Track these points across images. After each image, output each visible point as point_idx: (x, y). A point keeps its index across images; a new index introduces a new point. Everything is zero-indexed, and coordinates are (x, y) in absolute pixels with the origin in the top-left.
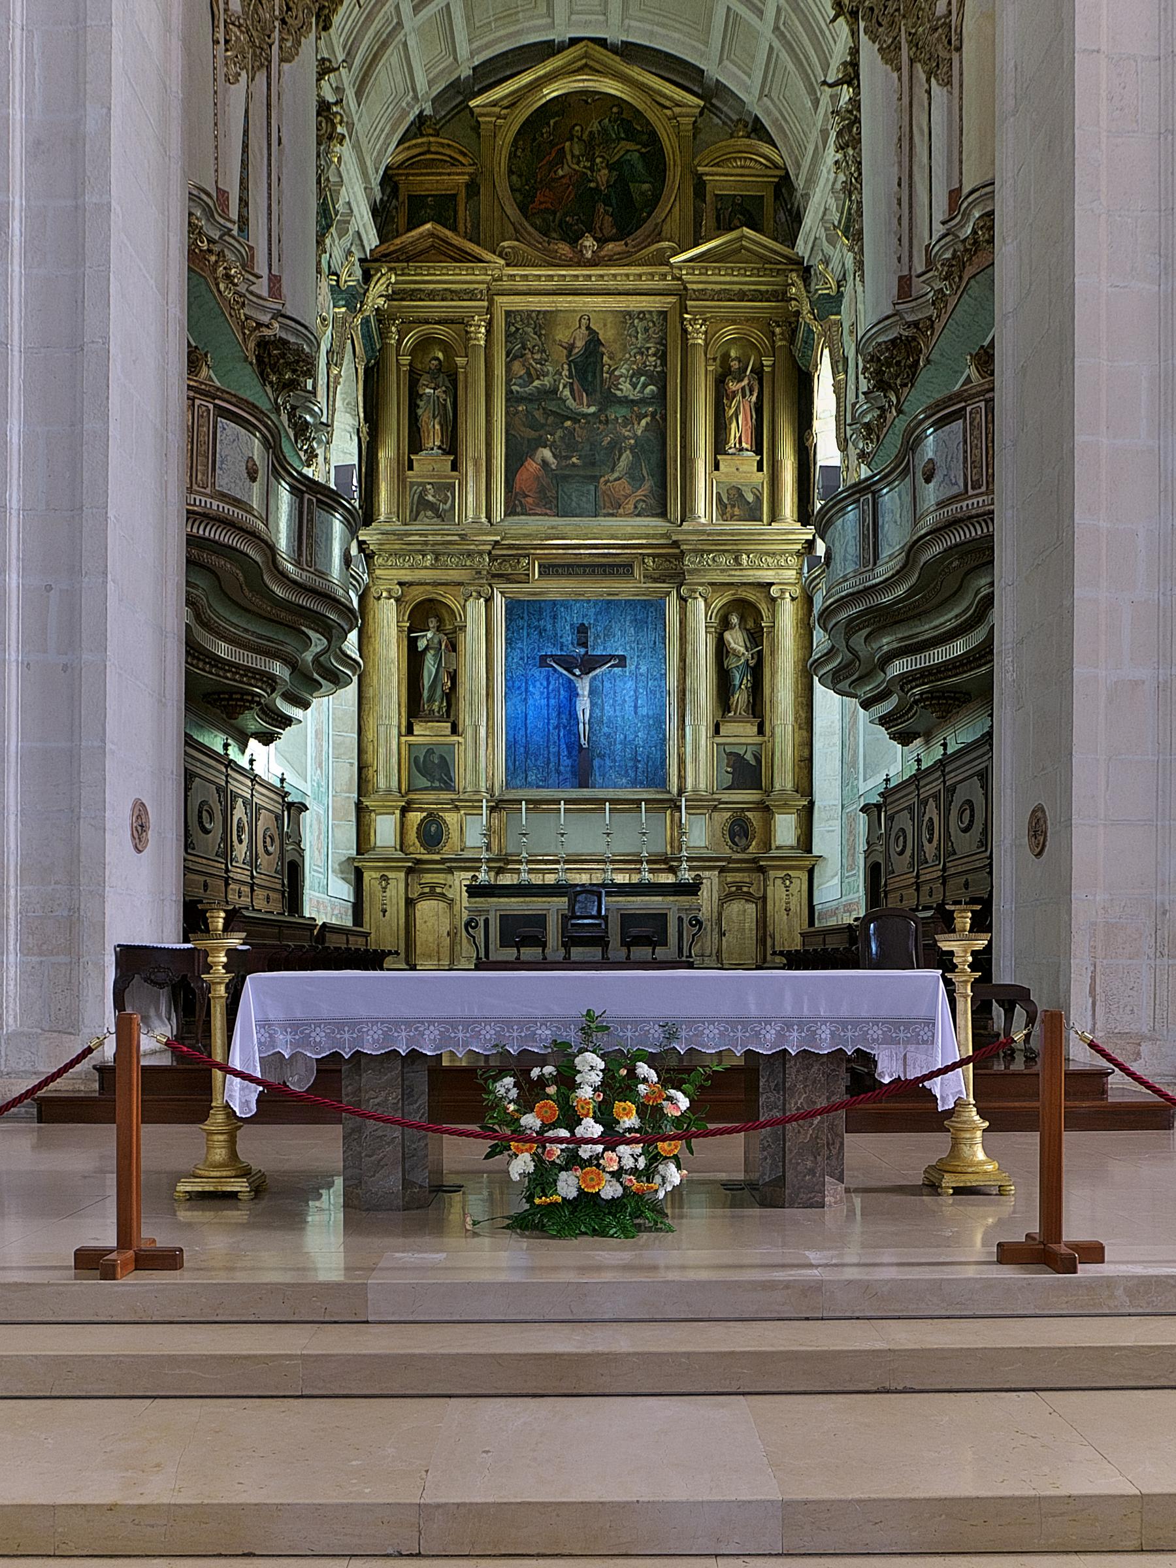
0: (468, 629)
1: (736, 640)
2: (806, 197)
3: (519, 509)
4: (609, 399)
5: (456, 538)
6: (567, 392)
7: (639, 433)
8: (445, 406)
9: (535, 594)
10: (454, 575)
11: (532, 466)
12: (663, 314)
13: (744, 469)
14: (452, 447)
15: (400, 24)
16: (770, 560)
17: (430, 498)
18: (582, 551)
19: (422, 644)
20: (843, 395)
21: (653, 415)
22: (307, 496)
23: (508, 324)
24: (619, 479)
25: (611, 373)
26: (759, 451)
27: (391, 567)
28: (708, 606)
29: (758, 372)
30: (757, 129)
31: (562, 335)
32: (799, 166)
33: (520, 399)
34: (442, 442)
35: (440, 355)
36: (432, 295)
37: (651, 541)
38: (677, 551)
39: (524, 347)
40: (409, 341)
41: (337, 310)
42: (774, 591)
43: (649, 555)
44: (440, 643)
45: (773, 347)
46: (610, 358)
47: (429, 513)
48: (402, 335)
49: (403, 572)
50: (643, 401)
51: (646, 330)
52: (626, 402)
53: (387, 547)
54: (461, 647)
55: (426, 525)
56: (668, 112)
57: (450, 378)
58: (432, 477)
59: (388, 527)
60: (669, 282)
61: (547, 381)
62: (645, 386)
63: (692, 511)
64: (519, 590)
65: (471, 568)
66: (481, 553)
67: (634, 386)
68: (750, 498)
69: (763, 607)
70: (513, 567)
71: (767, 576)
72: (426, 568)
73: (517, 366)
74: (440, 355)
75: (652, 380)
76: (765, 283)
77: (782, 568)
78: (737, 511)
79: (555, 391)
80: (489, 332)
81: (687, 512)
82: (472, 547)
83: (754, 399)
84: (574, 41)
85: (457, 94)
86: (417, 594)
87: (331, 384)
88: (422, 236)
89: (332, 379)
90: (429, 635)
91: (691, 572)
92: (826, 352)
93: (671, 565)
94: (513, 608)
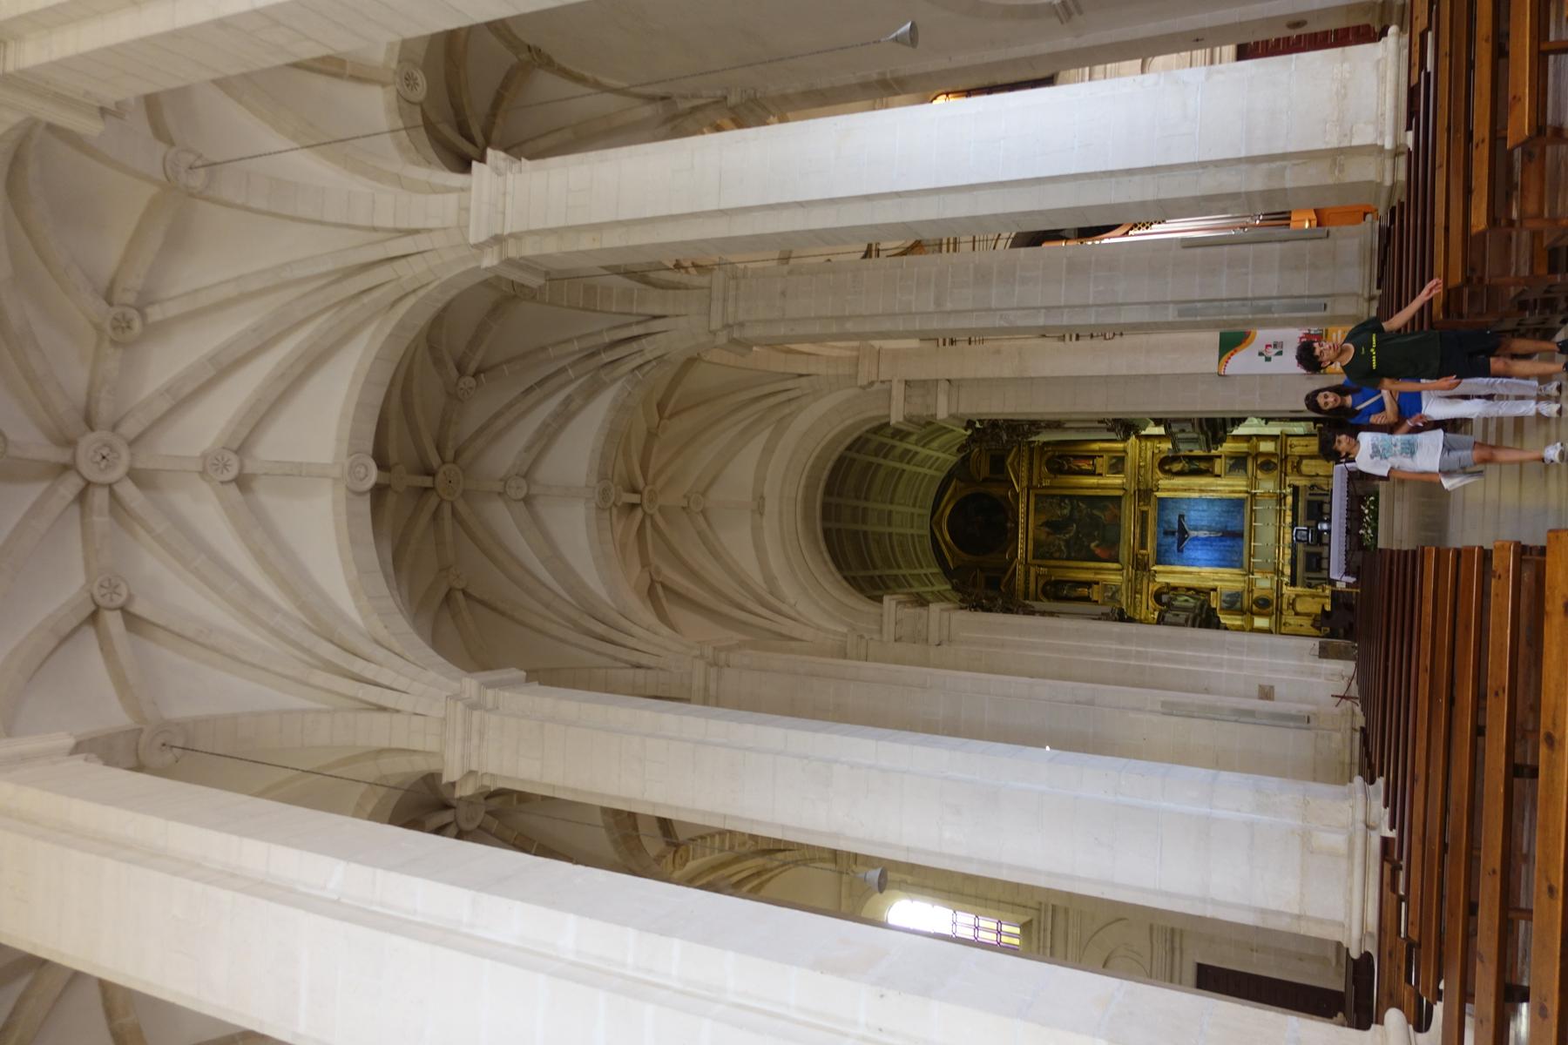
1: (1177, 467)
4: (1070, 519)
11: (1098, 551)
13: (1102, 464)
14: (1088, 584)
26: (1093, 457)
57: (1060, 583)
71: (1149, 454)
79: (1067, 542)
85: (948, 573)
94: (1158, 563)
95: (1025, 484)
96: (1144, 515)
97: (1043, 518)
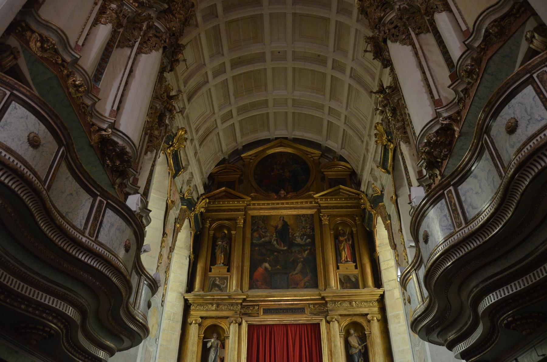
0: (231, 338)
1: (354, 341)
2: (362, 175)
3: (255, 287)
4: (291, 244)
5: (227, 297)
6: (275, 243)
7: (305, 256)
8: (226, 249)
9: (261, 321)
10: (225, 314)
11: (261, 270)
12: (312, 215)
13: (349, 269)
14: (228, 263)
15: (217, 127)
16: (365, 304)
17: (217, 282)
18: (282, 303)
19: (209, 345)
20: (390, 229)
21: (310, 250)
22: (99, 198)
23: (252, 220)
24: (297, 274)
25: (293, 235)
26: (354, 261)
27: (198, 310)
28: (340, 325)
29: (351, 233)
30: (342, 159)
31: (273, 223)
32: (357, 167)
33: (256, 245)
34: (224, 261)
35: (226, 232)
36: (224, 211)
37: (312, 297)
38: (324, 302)
39: (258, 227)
40: (214, 225)
41: (183, 207)
42: (369, 317)
43: (312, 304)
44: (217, 345)
45: (356, 225)
46: (292, 230)
47: (217, 289)
48: (211, 224)
49: (203, 312)
50: (306, 245)
51: (306, 220)
52: (299, 245)
53: (196, 302)
54: (226, 346)
55: (216, 294)
56: (310, 156)
57: (229, 239)
58: (219, 274)
59: (198, 293)
60: (314, 204)
61: (267, 239)
62: (306, 239)
63: (329, 285)
64: (255, 321)
65: (233, 310)
66: (237, 304)
67: (302, 239)
68: (354, 280)
69: (365, 324)
70: (252, 310)
71: (365, 311)
72: (213, 310)
73: (256, 234)
74: (226, 232)
75: (309, 237)
76: (349, 203)
77: (371, 307)
78: (348, 285)
79: (270, 242)
80: (244, 222)
81: (327, 284)
82: (234, 301)
83: (350, 243)
84: (276, 139)
85: (236, 153)
86: (208, 323)
87: (176, 230)
88: (221, 192)
89: (176, 229)
90: (213, 340)
91: (331, 310)
92: (380, 220)
93: (322, 307)
94: (251, 327)
95: (323, 203)
96: (300, 310)
97: (290, 222)
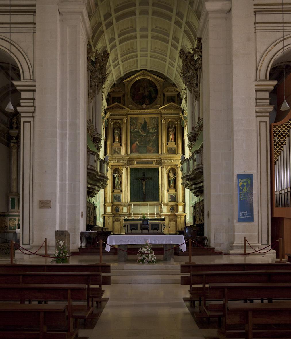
1: (171, 175)
4: (148, 133)
5: (121, 158)
6: (141, 131)
7: (154, 138)
11: (135, 145)
13: (172, 144)
14: (120, 141)
17: (116, 150)
21: (156, 135)
23: (130, 120)
24: (150, 147)
26: (175, 141)
28: (166, 169)
33: (132, 133)
36: (117, 115)
39: (133, 123)
40: (113, 122)
42: (178, 166)
46: (149, 125)
47: (116, 153)
48: (111, 122)
50: (154, 133)
51: (155, 120)
55: (116, 156)
57: (120, 129)
61: (137, 130)
62: (155, 130)
66: (126, 160)
67: (153, 130)
68: (174, 150)
69: (176, 169)
71: (176, 164)
73: (132, 127)
79: (138, 131)
83: (174, 132)
84: (141, 70)
86: (115, 167)
90: (117, 175)
93: (160, 162)
94: (131, 169)
